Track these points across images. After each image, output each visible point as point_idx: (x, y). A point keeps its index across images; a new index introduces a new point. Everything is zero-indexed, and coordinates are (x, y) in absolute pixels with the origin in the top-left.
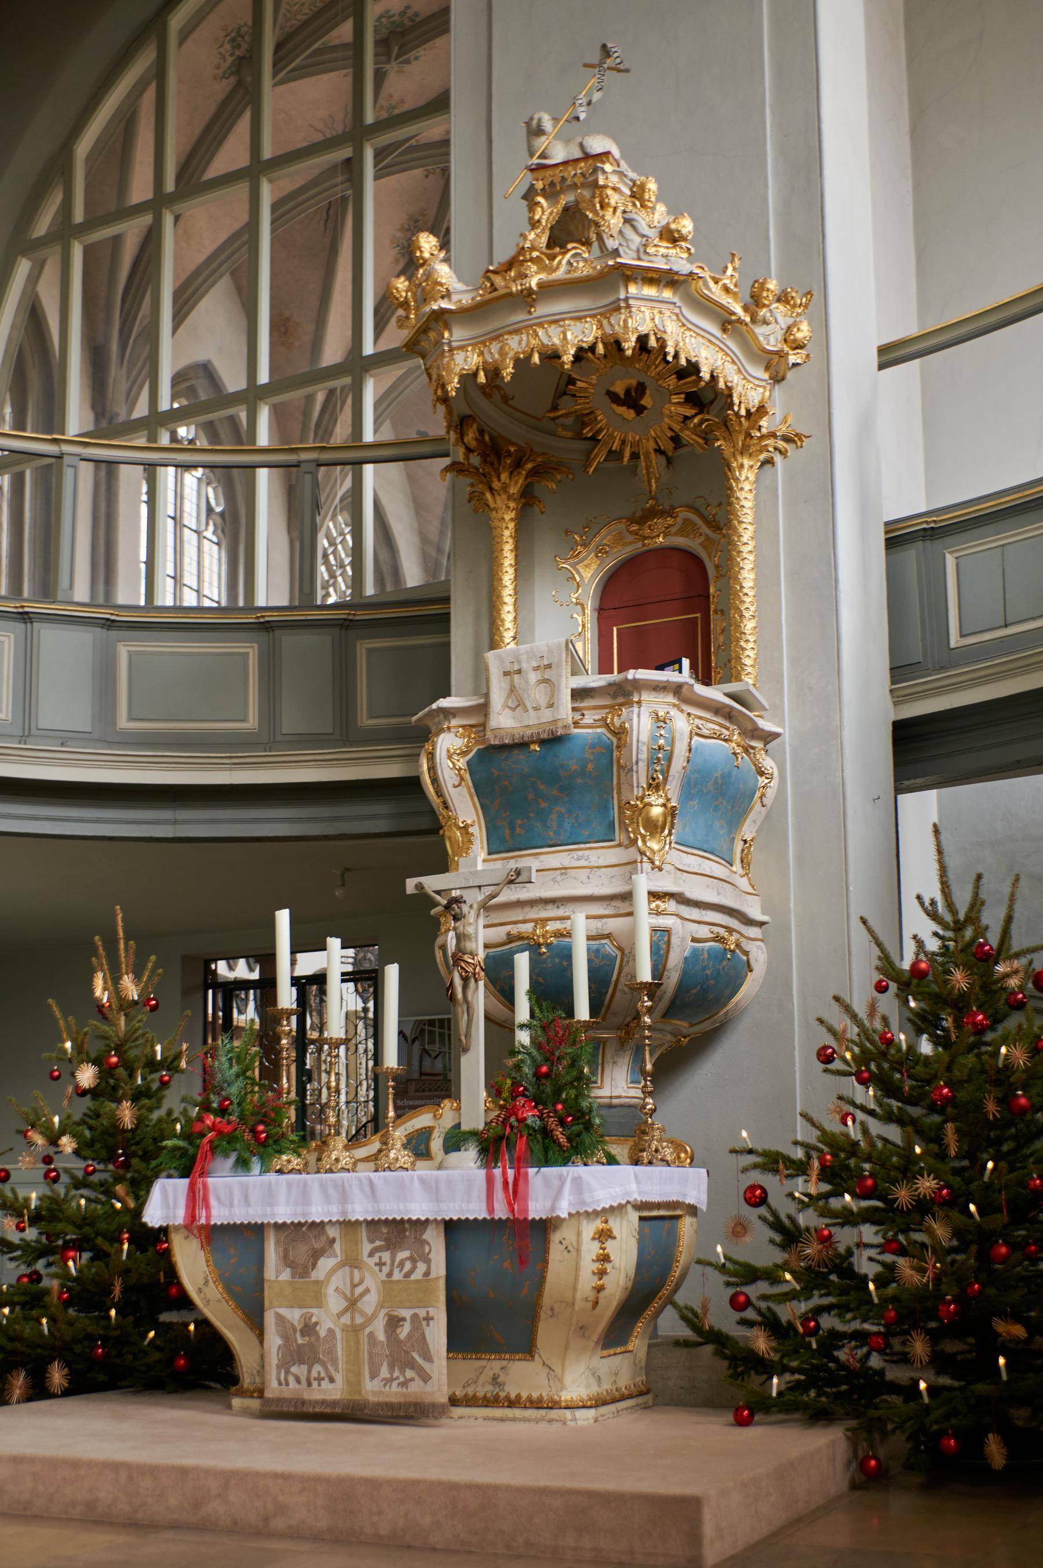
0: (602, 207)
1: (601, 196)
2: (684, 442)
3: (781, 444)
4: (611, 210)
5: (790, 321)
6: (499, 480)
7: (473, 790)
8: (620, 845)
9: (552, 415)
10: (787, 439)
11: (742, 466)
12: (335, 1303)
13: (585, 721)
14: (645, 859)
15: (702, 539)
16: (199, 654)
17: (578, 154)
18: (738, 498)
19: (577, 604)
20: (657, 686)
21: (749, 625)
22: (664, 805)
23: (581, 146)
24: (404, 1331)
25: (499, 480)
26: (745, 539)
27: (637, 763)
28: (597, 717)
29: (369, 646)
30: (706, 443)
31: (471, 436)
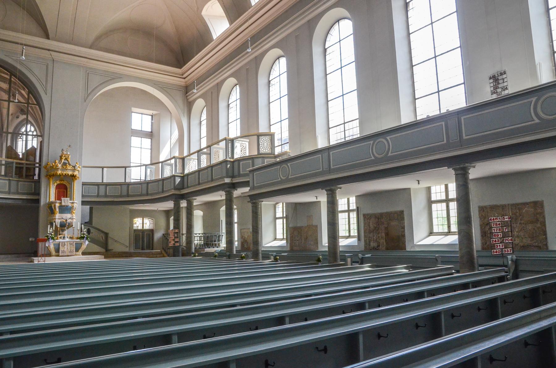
12: (66, 249)
24: (72, 250)
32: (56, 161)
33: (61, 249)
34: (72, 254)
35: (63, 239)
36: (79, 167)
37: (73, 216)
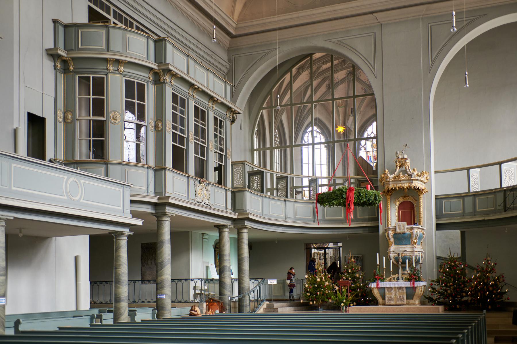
5: (426, 176)
12: (393, 295)
21: (422, 216)
24: (401, 297)
26: (421, 205)
32: (385, 171)
33: (387, 296)
34: (403, 303)
35: (396, 282)
37: (413, 248)
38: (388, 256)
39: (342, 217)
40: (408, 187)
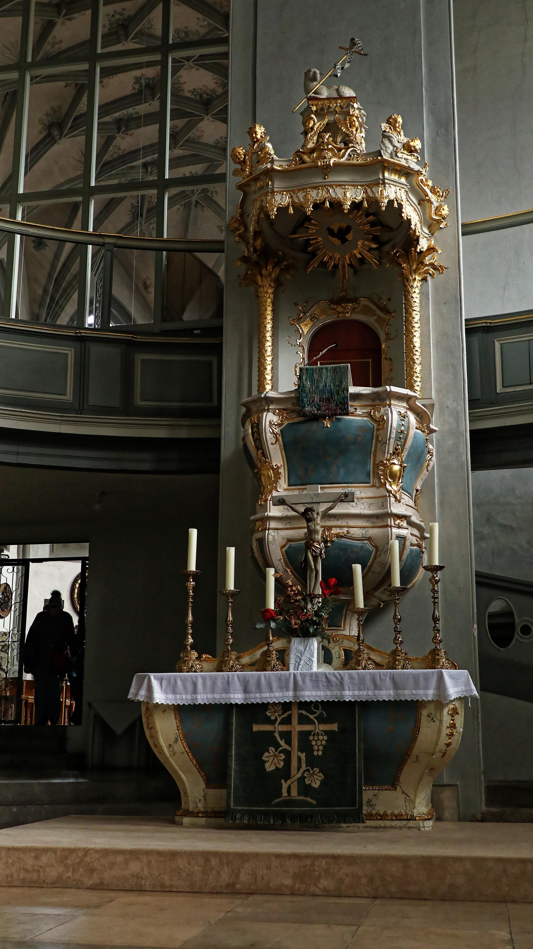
0: (350, 127)
1: (350, 119)
2: (366, 262)
3: (431, 271)
4: (355, 128)
6: (266, 269)
7: (282, 447)
8: (373, 486)
9: (291, 236)
10: (435, 268)
11: (415, 279)
13: (357, 413)
14: (391, 495)
15: (375, 318)
16: (44, 352)
17: (335, 95)
18: (412, 297)
19: (299, 346)
20: (400, 397)
22: (401, 465)
23: (338, 90)
25: (266, 269)
26: (415, 320)
27: (389, 439)
28: (364, 411)
29: (142, 357)
30: (380, 264)
31: (259, 242)
36: (410, 150)
37: (383, 500)
38: (255, 545)
39: (64, 394)
40: (361, 202)
